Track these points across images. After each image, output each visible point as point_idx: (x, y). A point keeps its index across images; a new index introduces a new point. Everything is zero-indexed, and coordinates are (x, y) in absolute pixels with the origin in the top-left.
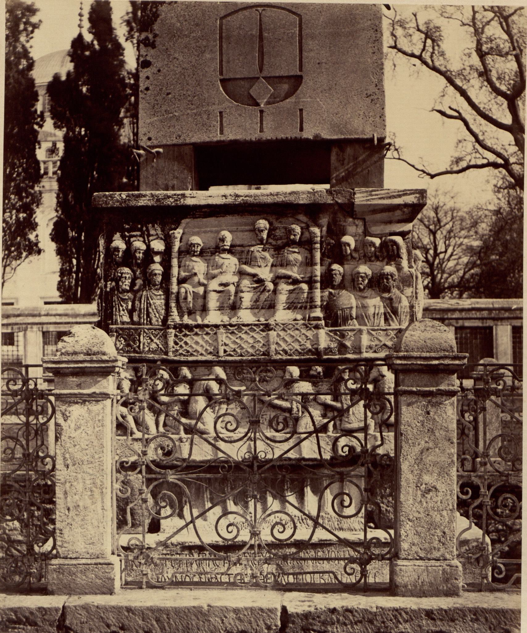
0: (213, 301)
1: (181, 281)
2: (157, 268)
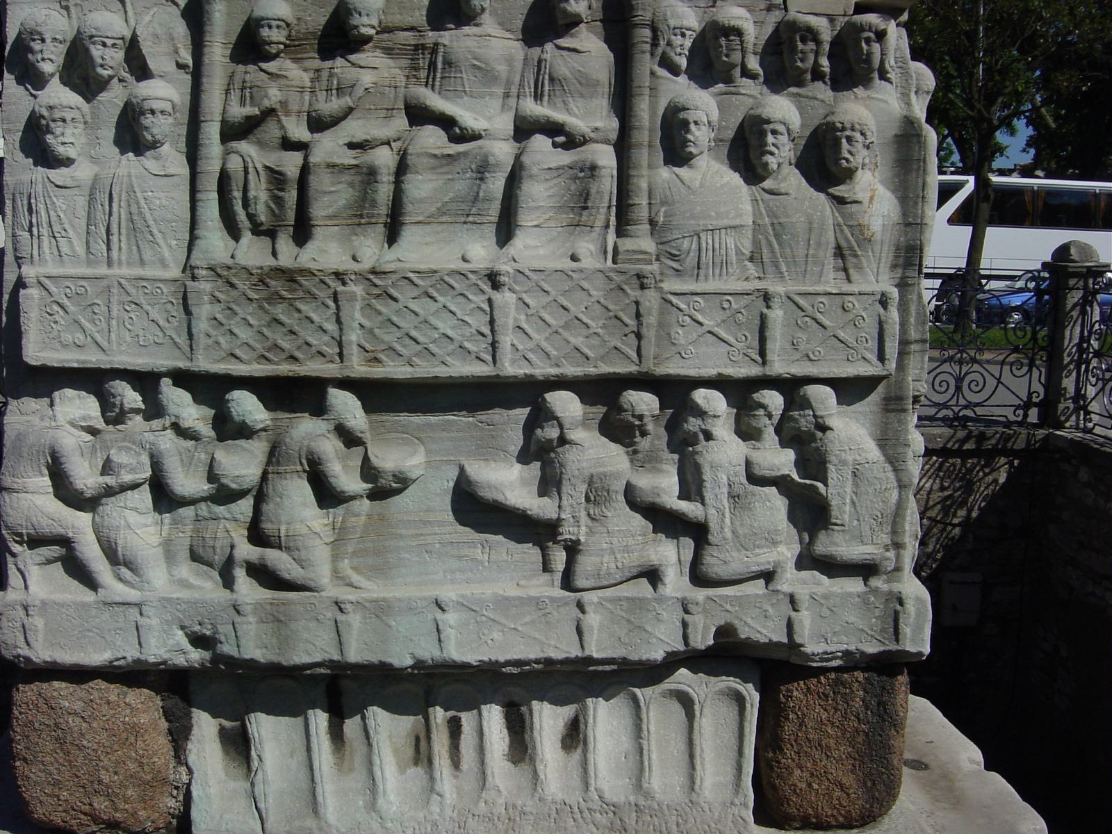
0: (332, 196)
1: (233, 132)
2: (164, 92)
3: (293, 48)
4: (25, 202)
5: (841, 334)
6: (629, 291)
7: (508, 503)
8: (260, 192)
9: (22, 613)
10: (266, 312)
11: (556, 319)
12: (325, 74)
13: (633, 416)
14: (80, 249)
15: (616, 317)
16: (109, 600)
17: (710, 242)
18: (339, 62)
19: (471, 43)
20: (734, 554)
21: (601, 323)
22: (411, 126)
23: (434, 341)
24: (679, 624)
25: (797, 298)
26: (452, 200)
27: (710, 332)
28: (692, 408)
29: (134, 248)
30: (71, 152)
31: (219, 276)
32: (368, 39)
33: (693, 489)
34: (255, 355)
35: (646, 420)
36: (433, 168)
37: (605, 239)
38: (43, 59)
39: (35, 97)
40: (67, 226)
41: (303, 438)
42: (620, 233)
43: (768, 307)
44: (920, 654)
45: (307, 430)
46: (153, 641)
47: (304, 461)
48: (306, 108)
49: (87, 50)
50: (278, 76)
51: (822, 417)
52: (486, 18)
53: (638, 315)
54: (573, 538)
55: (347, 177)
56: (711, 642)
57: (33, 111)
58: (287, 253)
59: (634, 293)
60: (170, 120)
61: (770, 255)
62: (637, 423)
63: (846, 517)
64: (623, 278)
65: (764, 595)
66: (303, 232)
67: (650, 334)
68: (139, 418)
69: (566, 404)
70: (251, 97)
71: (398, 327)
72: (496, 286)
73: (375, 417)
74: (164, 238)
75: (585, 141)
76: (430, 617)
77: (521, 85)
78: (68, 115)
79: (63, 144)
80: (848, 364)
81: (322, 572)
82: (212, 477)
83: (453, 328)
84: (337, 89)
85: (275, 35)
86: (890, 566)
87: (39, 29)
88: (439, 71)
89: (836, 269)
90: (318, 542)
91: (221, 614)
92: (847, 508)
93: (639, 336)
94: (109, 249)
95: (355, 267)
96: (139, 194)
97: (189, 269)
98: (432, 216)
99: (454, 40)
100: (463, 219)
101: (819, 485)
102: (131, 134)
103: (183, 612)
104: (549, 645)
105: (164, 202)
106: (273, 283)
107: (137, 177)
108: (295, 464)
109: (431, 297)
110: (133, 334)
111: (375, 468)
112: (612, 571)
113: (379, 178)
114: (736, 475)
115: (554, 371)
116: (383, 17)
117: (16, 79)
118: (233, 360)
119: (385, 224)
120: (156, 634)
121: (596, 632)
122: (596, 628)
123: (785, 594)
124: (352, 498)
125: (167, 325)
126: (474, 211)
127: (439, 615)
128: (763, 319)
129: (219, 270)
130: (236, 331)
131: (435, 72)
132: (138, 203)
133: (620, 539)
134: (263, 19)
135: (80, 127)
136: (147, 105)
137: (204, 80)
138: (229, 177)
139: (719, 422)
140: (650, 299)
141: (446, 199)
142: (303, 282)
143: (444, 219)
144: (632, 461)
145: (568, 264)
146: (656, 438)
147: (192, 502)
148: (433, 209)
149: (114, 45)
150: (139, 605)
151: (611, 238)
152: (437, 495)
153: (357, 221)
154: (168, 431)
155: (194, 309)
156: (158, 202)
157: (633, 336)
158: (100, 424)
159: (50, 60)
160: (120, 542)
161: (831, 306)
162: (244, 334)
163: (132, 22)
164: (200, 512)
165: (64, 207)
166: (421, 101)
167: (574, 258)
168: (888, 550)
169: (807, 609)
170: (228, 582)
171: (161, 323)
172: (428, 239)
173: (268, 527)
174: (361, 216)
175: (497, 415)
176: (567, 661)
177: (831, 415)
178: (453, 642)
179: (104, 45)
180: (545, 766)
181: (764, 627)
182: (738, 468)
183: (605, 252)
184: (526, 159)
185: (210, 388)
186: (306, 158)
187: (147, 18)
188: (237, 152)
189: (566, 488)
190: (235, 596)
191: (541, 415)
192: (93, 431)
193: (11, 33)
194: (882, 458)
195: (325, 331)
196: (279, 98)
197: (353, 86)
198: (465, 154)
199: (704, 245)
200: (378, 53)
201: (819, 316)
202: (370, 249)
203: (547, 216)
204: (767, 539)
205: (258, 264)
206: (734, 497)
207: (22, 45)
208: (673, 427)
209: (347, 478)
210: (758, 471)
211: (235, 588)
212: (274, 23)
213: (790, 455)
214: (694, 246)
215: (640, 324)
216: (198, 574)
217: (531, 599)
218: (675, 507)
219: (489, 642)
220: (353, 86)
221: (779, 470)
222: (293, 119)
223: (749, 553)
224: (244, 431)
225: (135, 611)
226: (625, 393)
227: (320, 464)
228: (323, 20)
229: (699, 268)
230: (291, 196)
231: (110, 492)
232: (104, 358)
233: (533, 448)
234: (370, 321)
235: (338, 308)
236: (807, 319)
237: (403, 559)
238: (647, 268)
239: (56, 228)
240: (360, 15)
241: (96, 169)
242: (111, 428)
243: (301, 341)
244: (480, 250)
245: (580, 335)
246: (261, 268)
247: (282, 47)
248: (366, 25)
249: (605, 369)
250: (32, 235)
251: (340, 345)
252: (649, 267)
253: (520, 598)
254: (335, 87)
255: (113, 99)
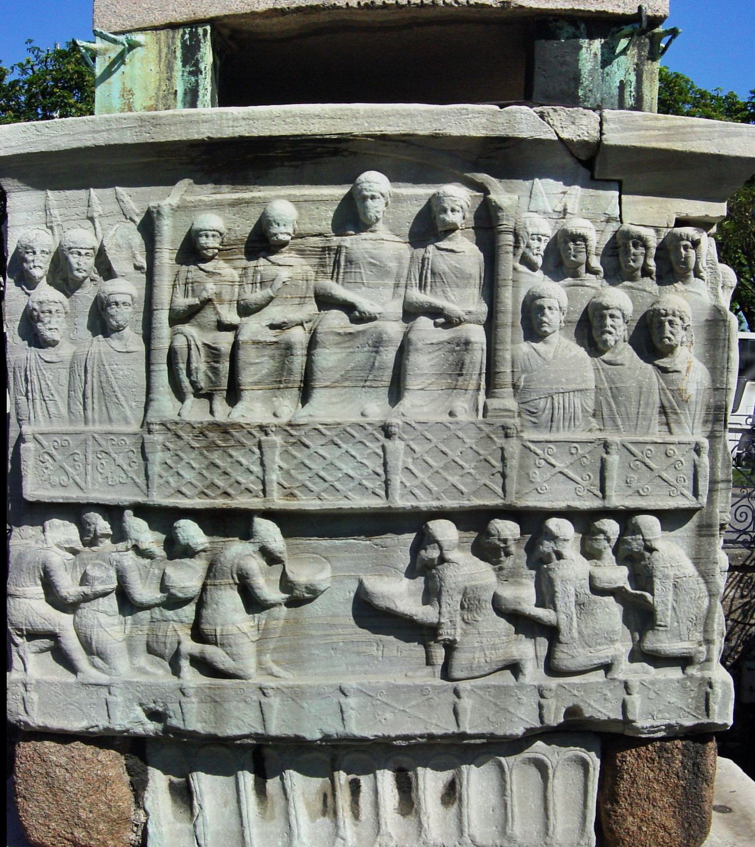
0: (256, 367)
1: (179, 318)
2: (126, 288)
3: (225, 251)
4: (23, 374)
5: (665, 475)
6: (496, 439)
7: (398, 610)
8: (200, 364)
9: (22, 689)
10: (206, 457)
11: (436, 462)
12: (250, 272)
13: (499, 540)
14: (64, 410)
15: (486, 460)
16: (86, 682)
17: (561, 402)
18: (262, 261)
19: (368, 245)
20: (580, 650)
21: (473, 465)
22: (319, 310)
23: (338, 480)
24: (536, 706)
25: (630, 447)
26: (353, 369)
27: (561, 472)
28: (546, 533)
29: (104, 408)
30: (56, 336)
31: (169, 430)
32: (284, 244)
33: (547, 598)
34: (197, 491)
35: (509, 543)
36: (338, 344)
37: (477, 400)
38: (34, 267)
39: (29, 295)
40: (53, 392)
42: (489, 394)
43: (607, 453)
44: (725, 725)
45: (237, 551)
46: (118, 714)
47: (235, 576)
48: (236, 298)
49: (67, 259)
50: (214, 273)
51: (649, 541)
52: (380, 226)
53: (503, 459)
54: (451, 638)
55: (268, 351)
56: (561, 720)
57: (28, 306)
58: (222, 412)
59: (500, 441)
60: (130, 309)
61: (609, 412)
62: (502, 545)
63: (669, 620)
64: (491, 429)
65: (604, 683)
66: (234, 395)
67: (513, 474)
68: (108, 542)
69: (445, 531)
70: (193, 290)
71: (310, 469)
72: (388, 435)
73: (291, 541)
74: (126, 401)
75: (460, 322)
76: (335, 700)
77: (409, 278)
78: (53, 309)
79: (50, 329)
80: (670, 498)
81: (249, 665)
82: (164, 588)
83: (354, 469)
84: (260, 283)
85: (212, 243)
86: (703, 657)
87: (31, 244)
88: (342, 267)
89: (661, 424)
90: (246, 640)
91: (171, 695)
92: (669, 613)
93: (504, 476)
94: (85, 409)
95: (275, 421)
96: (107, 367)
97: (146, 425)
98: (337, 381)
99: (353, 242)
100: (362, 384)
101: (648, 595)
102: (101, 321)
103: (141, 692)
104: (432, 724)
105: (126, 373)
106: (210, 435)
107: (105, 353)
108: (228, 578)
109: (336, 445)
110: (104, 476)
111: (291, 582)
112: (482, 664)
113: (294, 351)
114: (581, 587)
115: (435, 504)
116: (296, 226)
117: (15, 282)
118: (180, 495)
119: (300, 388)
120: (121, 709)
121: (469, 713)
122: (469, 710)
123: (620, 682)
124: (274, 605)
125: (129, 469)
126: (371, 377)
127: (342, 699)
128: (603, 462)
129: (169, 425)
130: (182, 472)
131: (339, 268)
132: (106, 374)
133: (487, 640)
134: (201, 230)
135: (62, 314)
136: (112, 299)
137: (156, 278)
138: (176, 353)
139: (568, 545)
140: (513, 447)
141: (349, 368)
142: (235, 433)
143: (346, 384)
144: (498, 576)
145: (446, 418)
146: (518, 557)
147: (149, 607)
148: (338, 376)
149: (86, 254)
150: (108, 686)
151: (482, 397)
152: (341, 603)
153: (277, 386)
154: (130, 552)
155: (150, 456)
156: (121, 373)
157: (499, 475)
158: (79, 545)
159: (39, 267)
160: (94, 637)
161: (656, 452)
162: (188, 475)
163: (100, 236)
164: (154, 615)
165: (51, 377)
166: (329, 290)
167: (451, 414)
168: (700, 645)
169: (638, 693)
170: (176, 670)
171: (125, 467)
172: (334, 400)
173: (206, 627)
174: (280, 382)
175: (390, 539)
176: (445, 736)
177: (656, 539)
178: (353, 721)
179: (80, 254)
180: (428, 818)
181: (604, 708)
182: (583, 581)
183: (477, 410)
184: (412, 336)
185: (162, 518)
186: (236, 336)
187: (112, 232)
188: (182, 333)
189: (445, 598)
190: (181, 681)
191: (424, 539)
192: (74, 552)
193: (11, 248)
194: (696, 573)
195: (251, 472)
196: (215, 291)
197: (273, 280)
198: (363, 332)
199: (556, 405)
200: (293, 254)
201: (647, 461)
202: (287, 407)
203: (430, 382)
204: (606, 638)
205: (199, 420)
206: (580, 605)
207: (19, 257)
208: (531, 548)
209: (269, 590)
210: (599, 584)
211: (182, 675)
212: (210, 233)
213: (624, 571)
214: (549, 405)
215: (504, 465)
216: (152, 664)
217: (416, 687)
218: (532, 613)
219: (383, 721)
220: (273, 280)
221: (616, 583)
222: (226, 306)
223: (592, 650)
224: (188, 552)
225: (104, 691)
226: (492, 521)
227: (248, 578)
228: (249, 230)
229: (552, 421)
230: (224, 367)
231: (86, 598)
232: (81, 494)
233: (418, 565)
234: (288, 463)
235: (262, 453)
236: (638, 463)
237: (313, 654)
238: (510, 422)
239: (46, 393)
240: (278, 225)
241: (74, 348)
242: (87, 549)
243: (232, 480)
244: (376, 407)
245: (456, 474)
246: (202, 423)
247: (216, 251)
248: (282, 232)
249: (477, 502)
250: (28, 399)
251: (264, 483)
252: (512, 421)
253: (408, 686)
254: (259, 281)
255: (86, 295)
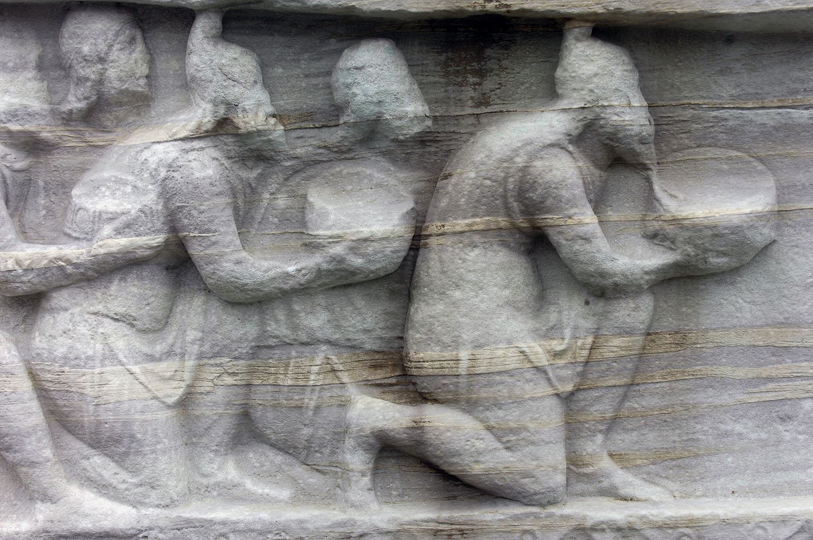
41: (516, 151)
237: (727, 434)
